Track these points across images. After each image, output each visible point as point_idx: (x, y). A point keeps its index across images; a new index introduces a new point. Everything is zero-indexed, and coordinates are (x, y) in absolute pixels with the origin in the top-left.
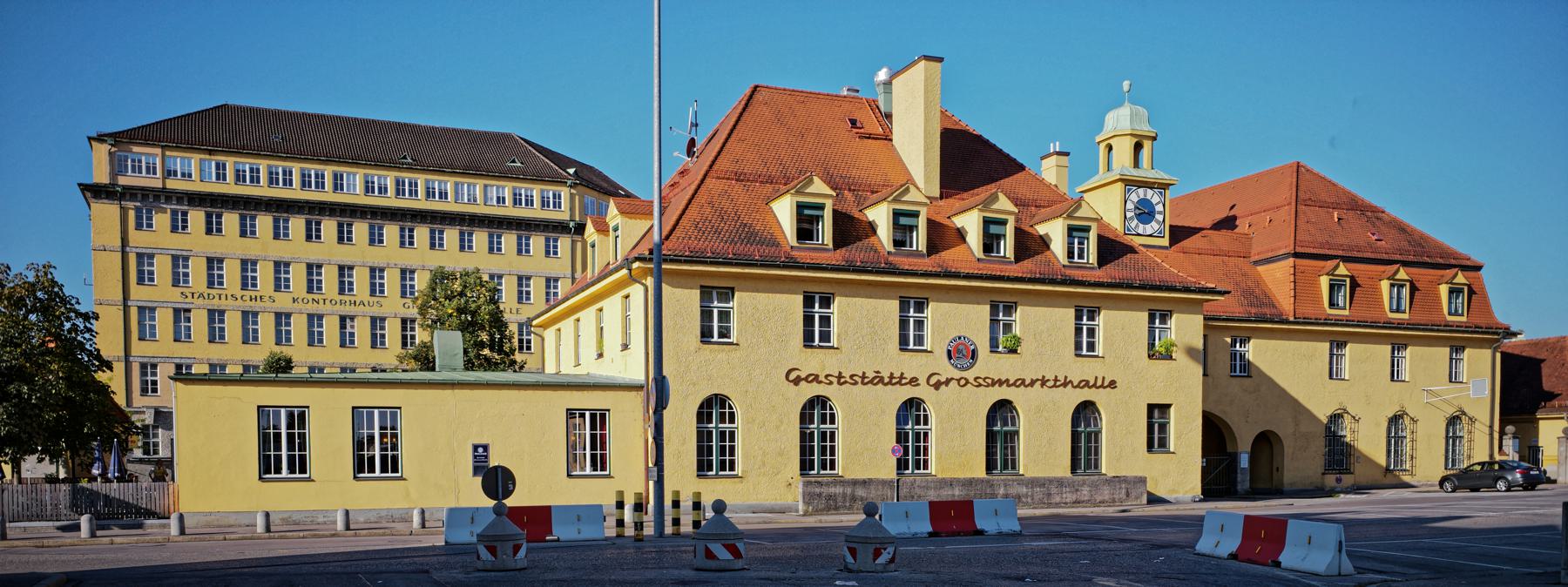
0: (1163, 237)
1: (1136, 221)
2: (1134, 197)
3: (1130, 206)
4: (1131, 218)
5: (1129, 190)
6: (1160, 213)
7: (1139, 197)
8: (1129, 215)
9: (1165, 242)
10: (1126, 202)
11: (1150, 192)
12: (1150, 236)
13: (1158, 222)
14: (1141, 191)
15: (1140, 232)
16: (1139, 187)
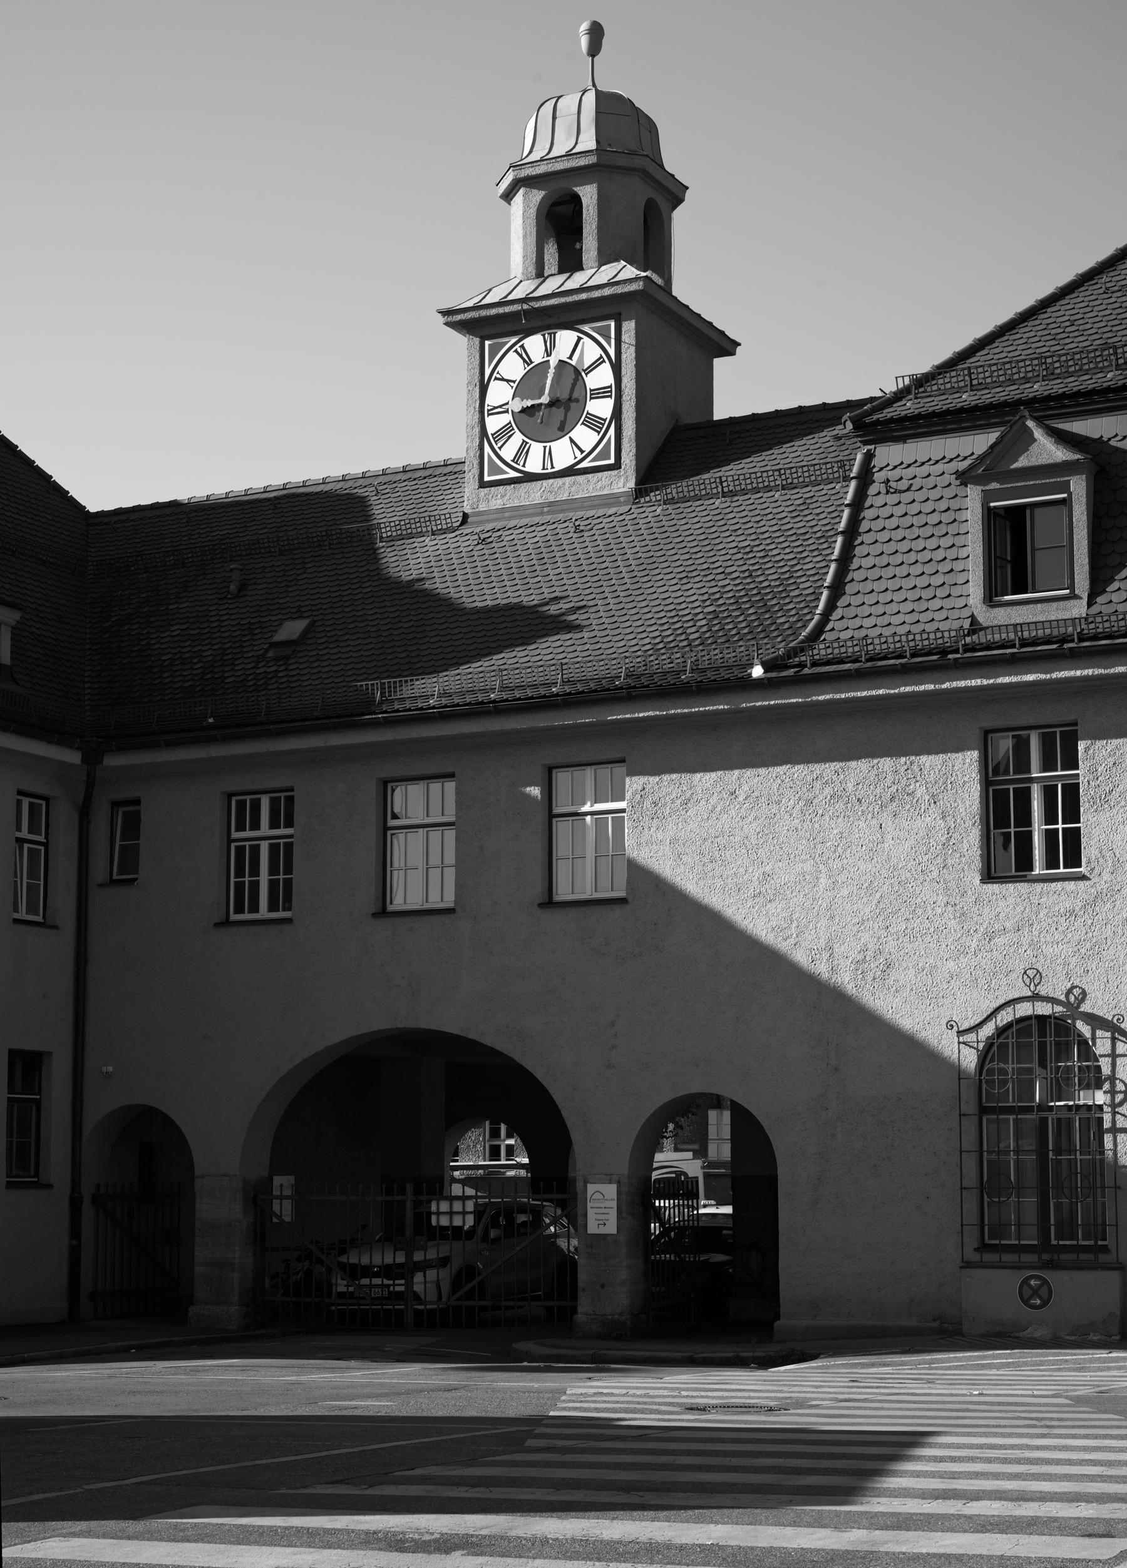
0: (617, 466)
1: (518, 438)
2: (512, 367)
3: (498, 394)
4: (505, 433)
5: (494, 351)
6: (600, 393)
7: (527, 361)
8: (494, 424)
9: (624, 482)
10: (484, 389)
11: (565, 339)
12: (570, 471)
13: (594, 423)
14: (535, 344)
15: (534, 465)
16: (528, 333)
